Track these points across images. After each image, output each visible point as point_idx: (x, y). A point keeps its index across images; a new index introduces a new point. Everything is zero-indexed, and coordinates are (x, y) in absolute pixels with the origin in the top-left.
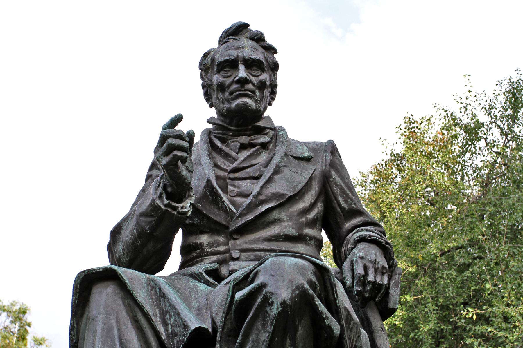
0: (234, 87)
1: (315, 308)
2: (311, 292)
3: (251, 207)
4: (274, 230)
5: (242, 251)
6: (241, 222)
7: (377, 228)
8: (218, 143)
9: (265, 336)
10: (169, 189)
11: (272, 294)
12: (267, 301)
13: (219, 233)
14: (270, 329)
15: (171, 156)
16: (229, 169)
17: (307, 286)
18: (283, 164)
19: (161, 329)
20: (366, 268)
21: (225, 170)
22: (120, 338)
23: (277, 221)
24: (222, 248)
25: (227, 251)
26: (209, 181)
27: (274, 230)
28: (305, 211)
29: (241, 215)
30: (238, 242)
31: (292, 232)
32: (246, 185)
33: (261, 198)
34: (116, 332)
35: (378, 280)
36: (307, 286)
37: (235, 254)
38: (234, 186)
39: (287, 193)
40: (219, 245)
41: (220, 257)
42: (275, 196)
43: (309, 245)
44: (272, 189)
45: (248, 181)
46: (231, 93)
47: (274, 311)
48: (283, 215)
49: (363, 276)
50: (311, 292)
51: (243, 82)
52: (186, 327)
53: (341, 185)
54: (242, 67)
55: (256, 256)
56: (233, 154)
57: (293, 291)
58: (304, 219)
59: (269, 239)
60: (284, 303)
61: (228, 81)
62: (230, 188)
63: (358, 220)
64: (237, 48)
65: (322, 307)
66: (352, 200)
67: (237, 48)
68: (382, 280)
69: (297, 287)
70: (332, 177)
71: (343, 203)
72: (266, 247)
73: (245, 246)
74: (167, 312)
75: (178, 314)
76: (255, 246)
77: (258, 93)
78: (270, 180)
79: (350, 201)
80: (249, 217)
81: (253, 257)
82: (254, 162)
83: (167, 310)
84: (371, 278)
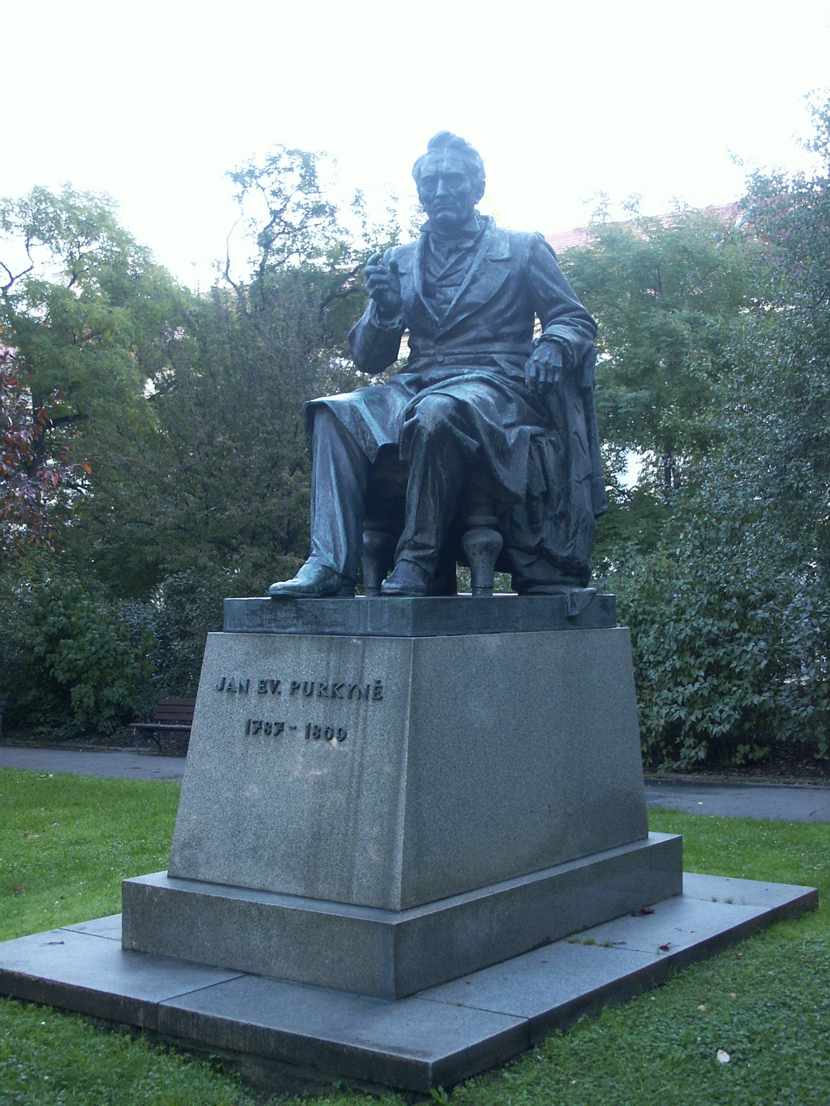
0: (437, 201)
1: (453, 435)
2: (450, 424)
3: (452, 317)
4: (472, 335)
5: (445, 355)
6: (442, 331)
7: (578, 313)
8: (432, 245)
10: (382, 310)
11: (422, 427)
12: (419, 433)
14: (424, 451)
15: (374, 289)
16: (438, 275)
17: (446, 420)
18: (480, 272)
19: (362, 443)
20: (538, 371)
21: (435, 276)
22: (333, 453)
23: (472, 327)
24: (432, 352)
25: (434, 355)
26: (417, 295)
27: (472, 335)
28: (501, 313)
29: (443, 326)
30: (442, 347)
31: (488, 334)
32: (450, 291)
33: (458, 309)
34: (330, 449)
35: (549, 380)
36: (446, 420)
37: (440, 359)
38: (441, 293)
39: (481, 301)
42: (471, 305)
43: (506, 341)
44: (469, 299)
45: (453, 288)
47: (424, 439)
48: (480, 321)
49: (534, 378)
50: (450, 424)
52: (376, 444)
53: (540, 279)
55: (456, 359)
56: (442, 259)
57: (436, 425)
58: (500, 320)
60: (429, 434)
62: (438, 295)
63: (560, 307)
65: (460, 433)
66: (553, 291)
68: (553, 379)
69: (439, 422)
70: (530, 272)
71: (543, 295)
72: (464, 351)
73: (447, 351)
74: (365, 432)
75: (372, 434)
76: (456, 351)
77: (458, 204)
78: (467, 291)
79: (550, 292)
81: (454, 360)
82: (460, 267)
83: (366, 432)
84: (542, 378)
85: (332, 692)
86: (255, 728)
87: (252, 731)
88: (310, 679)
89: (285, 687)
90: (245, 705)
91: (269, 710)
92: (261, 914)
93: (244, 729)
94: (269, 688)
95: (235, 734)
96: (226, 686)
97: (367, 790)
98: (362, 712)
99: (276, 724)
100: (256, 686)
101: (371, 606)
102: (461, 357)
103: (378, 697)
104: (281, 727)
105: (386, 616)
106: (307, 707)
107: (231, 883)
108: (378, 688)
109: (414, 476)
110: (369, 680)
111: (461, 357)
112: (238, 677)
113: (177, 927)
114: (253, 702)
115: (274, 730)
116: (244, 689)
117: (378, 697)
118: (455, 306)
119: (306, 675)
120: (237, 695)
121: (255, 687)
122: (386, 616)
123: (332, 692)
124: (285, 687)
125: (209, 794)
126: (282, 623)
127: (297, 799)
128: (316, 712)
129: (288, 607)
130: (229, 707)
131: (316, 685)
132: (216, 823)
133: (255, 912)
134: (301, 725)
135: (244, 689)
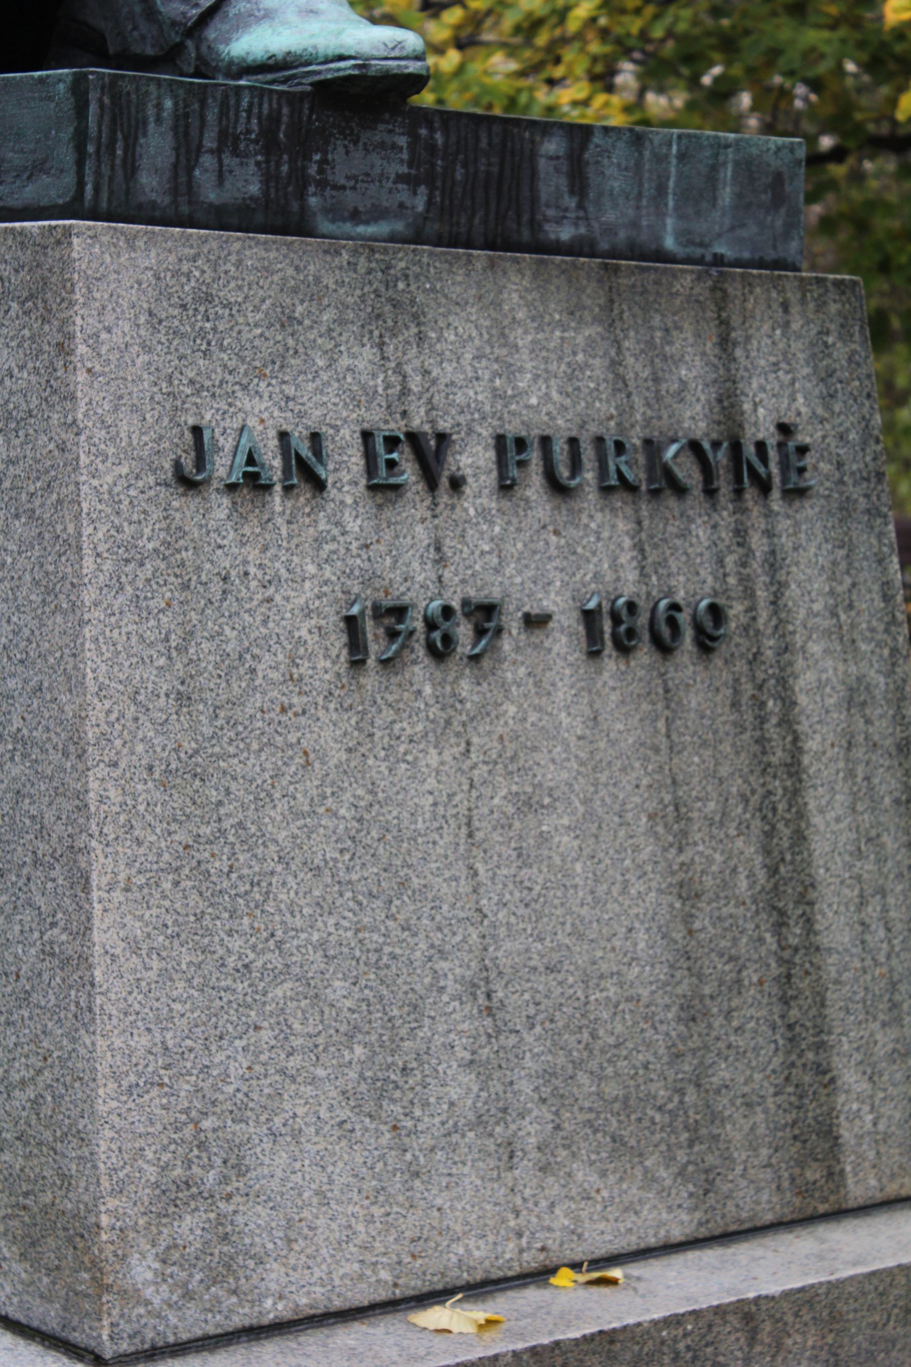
85: (643, 476)
86: (377, 632)
87: (376, 645)
88: (562, 427)
89: (474, 459)
90: (319, 541)
91: (421, 554)
93: (338, 642)
95: (304, 668)
96: (223, 466)
97: (821, 811)
98: (758, 543)
101: (682, 157)
104: (484, 614)
105: (726, 195)
106: (572, 532)
107: (414, 1285)
110: (760, 424)
112: (255, 419)
114: (353, 526)
115: (464, 631)
116: (306, 472)
122: (726, 195)
125: (236, 944)
126: (350, 199)
127: (602, 888)
129: (379, 134)
130: (253, 554)
131: (588, 454)
132: (294, 1062)
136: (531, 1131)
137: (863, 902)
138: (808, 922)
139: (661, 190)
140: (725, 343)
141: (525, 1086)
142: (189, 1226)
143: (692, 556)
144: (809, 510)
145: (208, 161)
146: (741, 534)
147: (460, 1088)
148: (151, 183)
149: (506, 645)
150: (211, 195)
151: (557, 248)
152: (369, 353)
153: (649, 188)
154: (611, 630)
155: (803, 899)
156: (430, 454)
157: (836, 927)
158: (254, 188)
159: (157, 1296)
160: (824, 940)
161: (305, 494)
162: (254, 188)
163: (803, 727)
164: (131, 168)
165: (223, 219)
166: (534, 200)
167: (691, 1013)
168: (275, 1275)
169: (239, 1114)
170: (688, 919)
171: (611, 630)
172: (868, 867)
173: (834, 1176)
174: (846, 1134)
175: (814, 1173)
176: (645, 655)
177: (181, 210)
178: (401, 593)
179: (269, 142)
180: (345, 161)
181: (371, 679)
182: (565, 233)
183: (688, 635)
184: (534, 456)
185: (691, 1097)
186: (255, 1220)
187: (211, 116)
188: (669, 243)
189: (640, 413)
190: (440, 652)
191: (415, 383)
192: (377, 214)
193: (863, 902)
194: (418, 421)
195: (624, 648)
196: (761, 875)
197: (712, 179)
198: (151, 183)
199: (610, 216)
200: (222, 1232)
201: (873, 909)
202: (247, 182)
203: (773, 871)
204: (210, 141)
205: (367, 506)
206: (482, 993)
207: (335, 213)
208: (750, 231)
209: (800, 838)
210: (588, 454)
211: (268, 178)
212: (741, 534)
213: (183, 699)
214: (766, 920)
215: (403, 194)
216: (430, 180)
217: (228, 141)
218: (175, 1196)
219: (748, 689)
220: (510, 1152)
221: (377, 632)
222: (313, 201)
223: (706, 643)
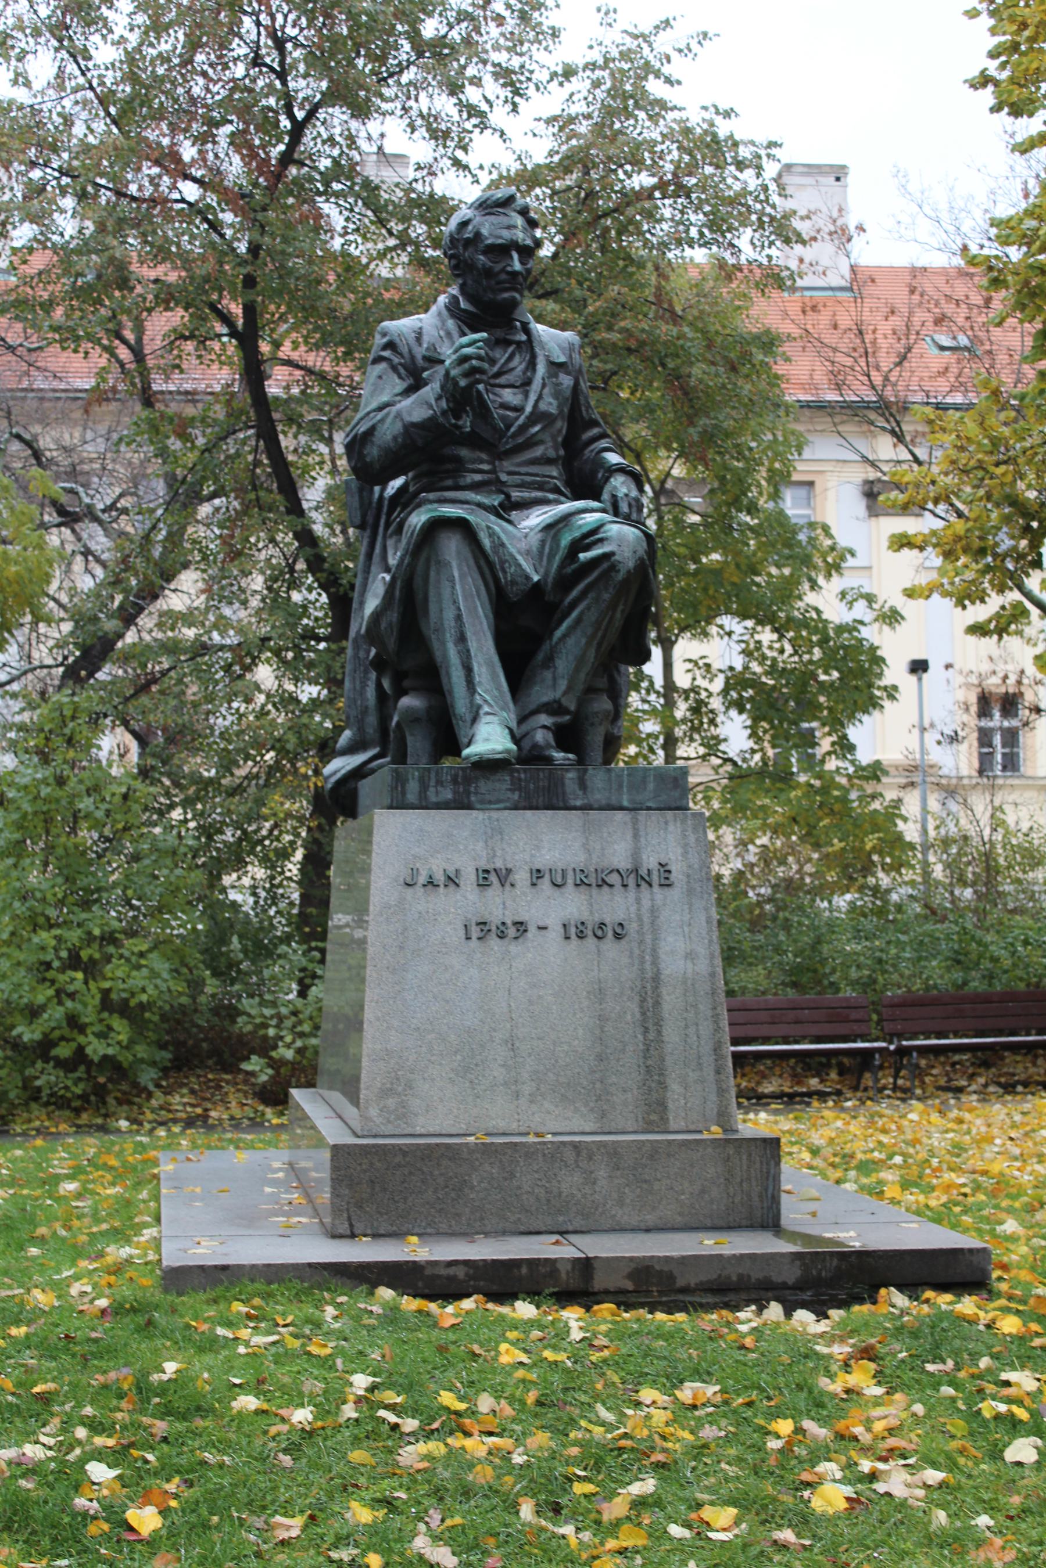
0: (503, 276)
4: (538, 452)
5: (510, 473)
9: (606, 596)
13: (481, 449)
23: (541, 442)
24: (486, 467)
27: (538, 452)
40: (482, 462)
41: (486, 477)
46: (499, 283)
47: (620, 576)
51: (515, 274)
52: (528, 578)
54: (515, 256)
59: (534, 462)
61: (498, 267)
64: (509, 227)
67: (509, 227)
76: (523, 470)
80: (520, 440)
82: (511, 365)
85: (595, 880)
88: (560, 866)
89: (522, 877)
91: (497, 905)
92: (578, 1154)
93: (462, 933)
94: (493, 878)
96: (422, 879)
98: (646, 903)
99: (515, 924)
100: (473, 877)
102: (528, 479)
103: (667, 885)
104: (521, 926)
105: (651, 786)
108: (665, 869)
109: (579, 621)
111: (528, 479)
112: (438, 867)
113: (435, 1191)
114: (470, 897)
116: (452, 881)
117: (667, 885)
118: (532, 413)
119: (549, 857)
120: (442, 889)
121: (469, 878)
122: (651, 786)
123: (595, 880)
124: (522, 877)
126: (487, 797)
128: (572, 905)
129: (498, 776)
131: (570, 874)
133: (569, 1155)
134: (554, 922)
135: (452, 881)
136: (527, 1089)
137: (686, 1027)
138: (659, 1032)
139: (621, 786)
140: (636, 836)
141: (526, 1075)
142: (391, 1102)
143: (616, 906)
144: (675, 894)
145: (432, 789)
146: (638, 901)
147: (499, 1073)
148: (411, 797)
149: (529, 935)
150: (433, 798)
151: (575, 808)
152: (481, 844)
153: (614, 786)
154: (577, 931)
155: (657, 1024)
156: (504, 877)
157: (671, 1034)
158: (450, 796)
159: (378, 1120)
160: (666, 1039)
161: (452, 887)
162: (450, 796)
163: (662, 965)
164: (404, 793)
165: (438, 806)
166: (564, 793)
167: (600, 1058)
168: (421, 1120)
169: (412, 1071)
170: (602, 1028)
171: (577, 931)
172: (691, 1015)
173: (664, 1119)
174: (671, 1105)
175: (654, 1117)
176: (591, 941)
177: (424, 804)
178: (487, 918)
179: (455, 781)
180: (484, 786)
181: (474, 943)
182: (578, 803)
183: (610, 934)
184: (547, 877)
185: (598, 1085)
186: (415, 1103)
187: (433, 775)
188: (625, 803)
189: (595, 859)
190: (502, 936)
191: (499, 853)
192: (499, 801)
193: (686, 1027)
194: (499, 864)
195: (581, 936)
196: (638, 1016)
197: (644, 781)
198: (411, 797)
199: (598, 796)
200: (403, 1105)
201: (692, 1030)
202: (448, 794)
203: (643, 1014)
204: (432, 783)
205: (477, 889)
206: (511, 1043)
207: (482, 802)
208: (664, 797)
209: (657, 1003)
210: (570, 874)
211: (455, 792)
212: (638, 901)
213: (401, 948)
214: (639, 1030)
215: (509, 794)
216: (520, 789)
217: (439, 783)
218: (386, 1092)
219: (637, 952)
220: (517, 1095)
221: (483, 929)
222: (473, 798)
223: (618, 936)
